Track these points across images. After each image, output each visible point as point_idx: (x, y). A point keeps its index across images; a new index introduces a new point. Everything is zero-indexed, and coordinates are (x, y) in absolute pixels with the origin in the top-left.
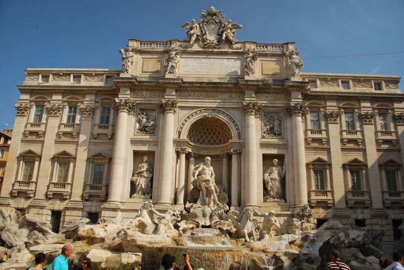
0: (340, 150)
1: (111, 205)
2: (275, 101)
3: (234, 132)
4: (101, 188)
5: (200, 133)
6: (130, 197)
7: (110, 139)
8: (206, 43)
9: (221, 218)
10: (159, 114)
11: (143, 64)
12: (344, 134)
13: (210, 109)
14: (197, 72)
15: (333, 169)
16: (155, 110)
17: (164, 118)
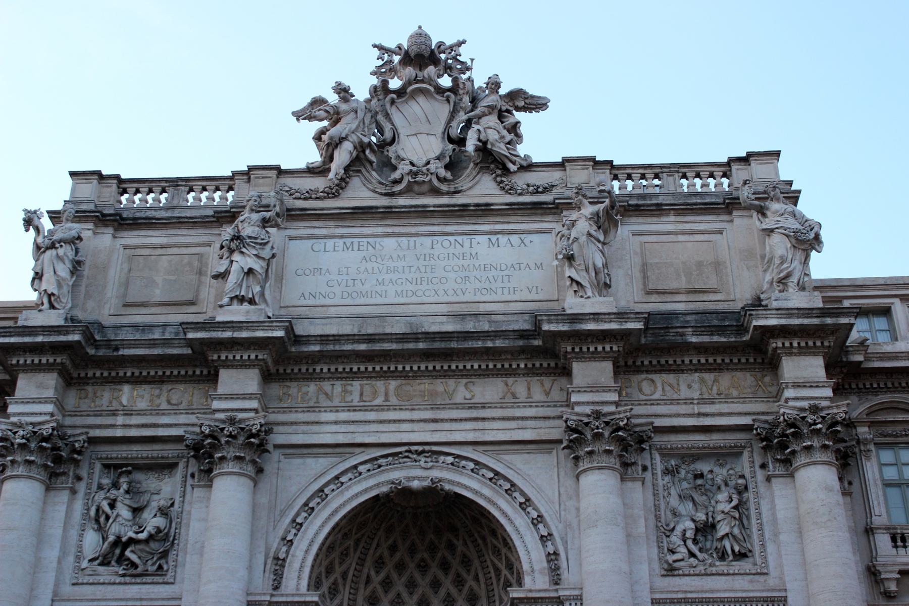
3: (529, 552)
5: (379, 564)
8: (396, 175)
10: (190, 481)
11: (130, 270)
13: (419, 453)
14: (361, 294)
16: (172, 466)
17: (209, 499)
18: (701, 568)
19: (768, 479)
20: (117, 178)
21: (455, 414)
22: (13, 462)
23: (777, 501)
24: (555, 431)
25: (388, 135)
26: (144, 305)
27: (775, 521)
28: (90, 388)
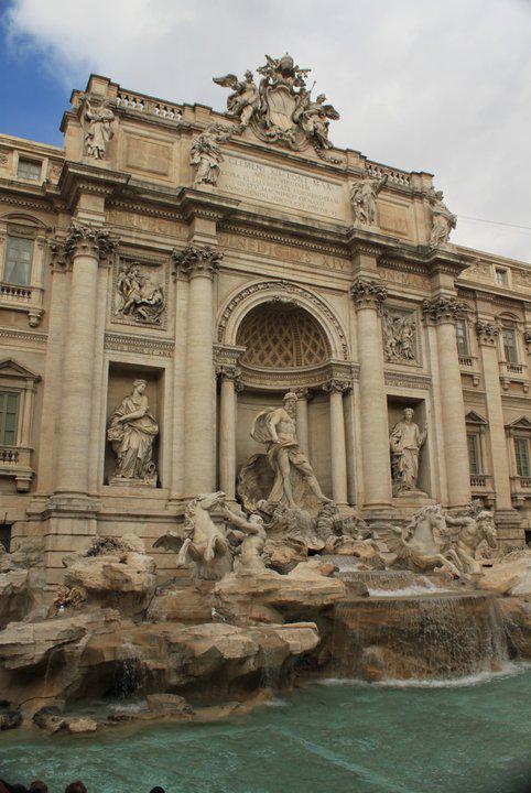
0: (500, 399)
1: (75, 502)
2: (407, 287)
3: (335, 343)
4: (17, 455)
5: (247, 336)
6: (106, 483)
7: (34, 326)
9: (338, 530)
11: (128, 146)
12: (504, 368)
15: (492, 435)
18: (398, 361)
19: (425, 327)
20: (118, 86)
21: (303, 268)
22: (84, 247)
23: (430, 338)
24: (345, 286)
25: (264, 108)
26: (138, 169)
27: (428, 345)
28: (113, 212)
